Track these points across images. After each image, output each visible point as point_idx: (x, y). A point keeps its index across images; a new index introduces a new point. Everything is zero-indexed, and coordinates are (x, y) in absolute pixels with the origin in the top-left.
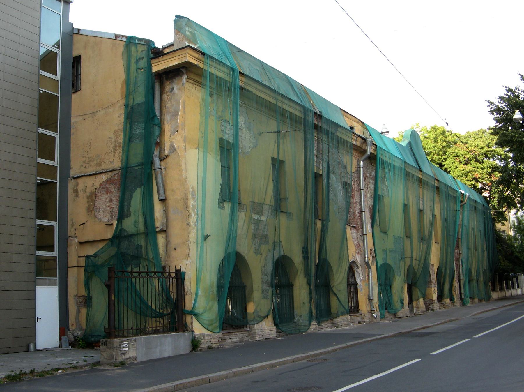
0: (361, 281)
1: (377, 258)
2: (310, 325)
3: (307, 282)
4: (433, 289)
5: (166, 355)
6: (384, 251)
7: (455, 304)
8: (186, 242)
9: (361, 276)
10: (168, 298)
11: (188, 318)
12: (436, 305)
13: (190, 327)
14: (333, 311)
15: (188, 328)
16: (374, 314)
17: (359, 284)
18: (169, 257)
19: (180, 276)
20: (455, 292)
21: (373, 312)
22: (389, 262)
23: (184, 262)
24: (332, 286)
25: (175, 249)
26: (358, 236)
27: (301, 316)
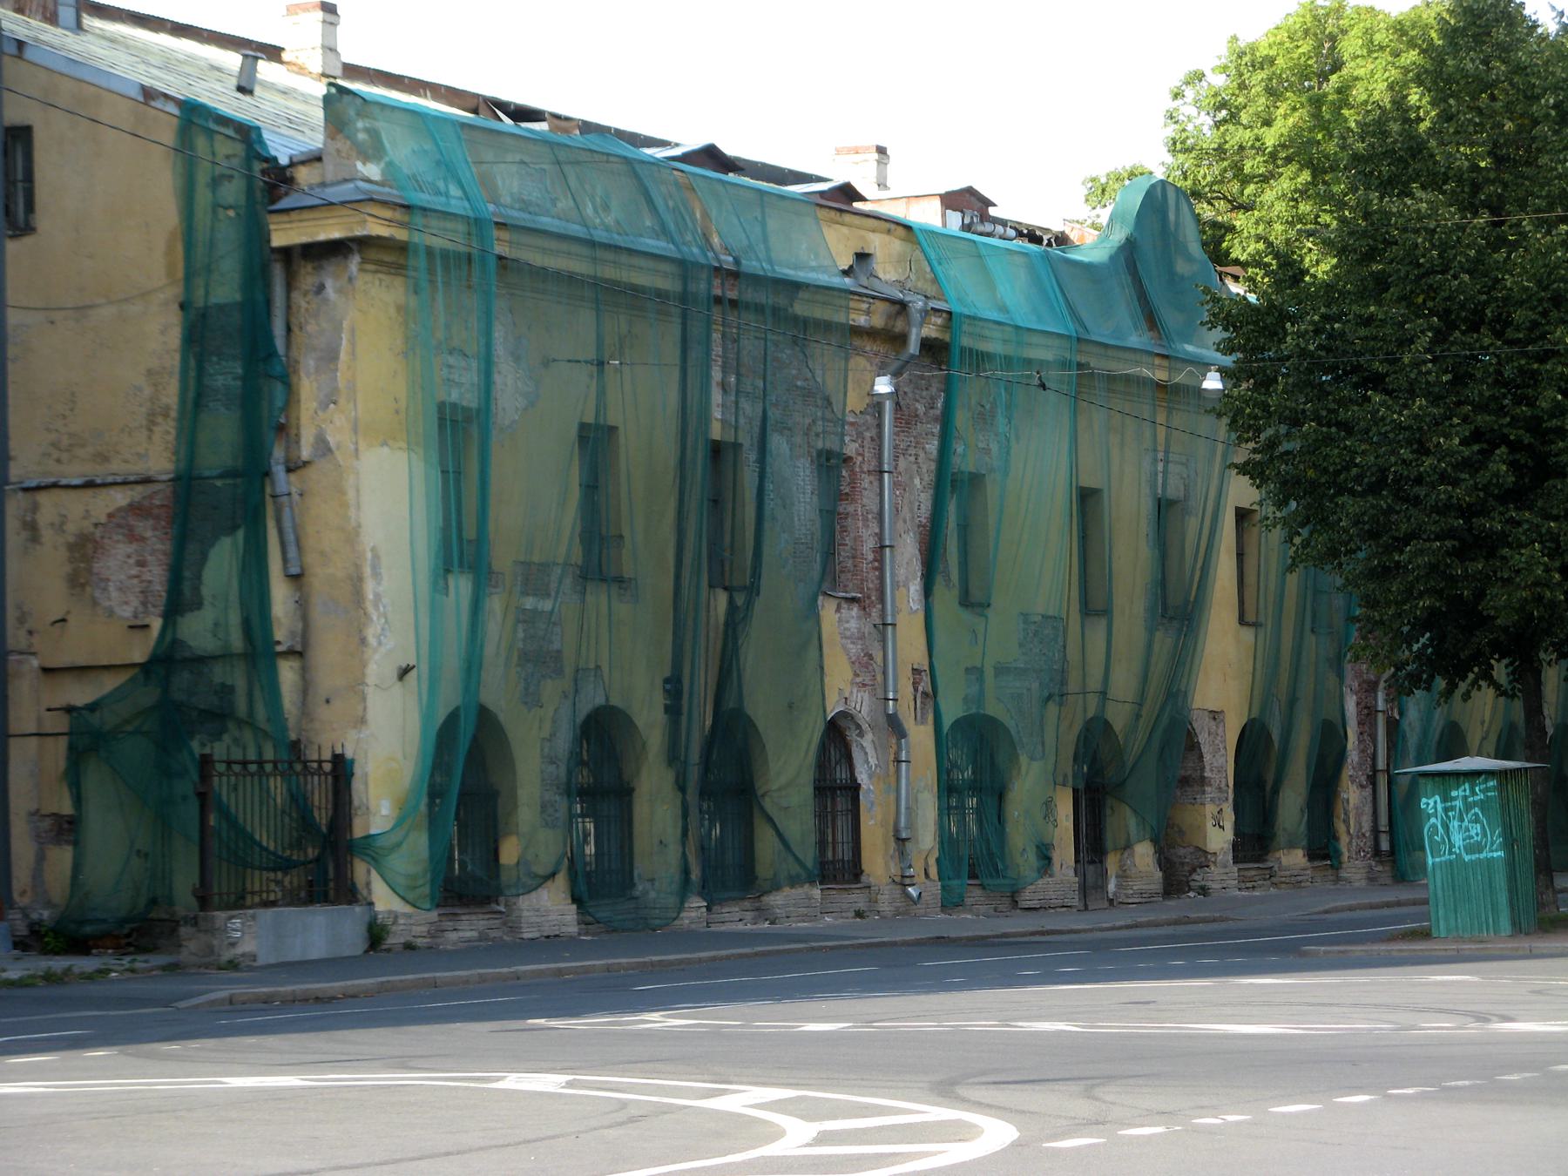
0: (870, 777)
1: (938, 699)
2: (681, 908)
3: (677, 781)
4: (1210, 809)
5: (314, 955)
6: (975, 672)
7: (1343, 874)
8: (357, 687)
9: (873, 761)
10: (305, 821)
11: (360, 869)
12: (1222, 874)
13: (365, 892)
14: (763, 870)
15: (359, 896)
16: (910, 889)
17: (864, 786)
18: (312, 720)
19: (341, 769)
20: (1347, 822)
21: (907, 881)
22: (993, 709)
23: (352, 735)
24: (760, 793)
25: (328, 701)
26: (868, 629)
27: (652, 880)
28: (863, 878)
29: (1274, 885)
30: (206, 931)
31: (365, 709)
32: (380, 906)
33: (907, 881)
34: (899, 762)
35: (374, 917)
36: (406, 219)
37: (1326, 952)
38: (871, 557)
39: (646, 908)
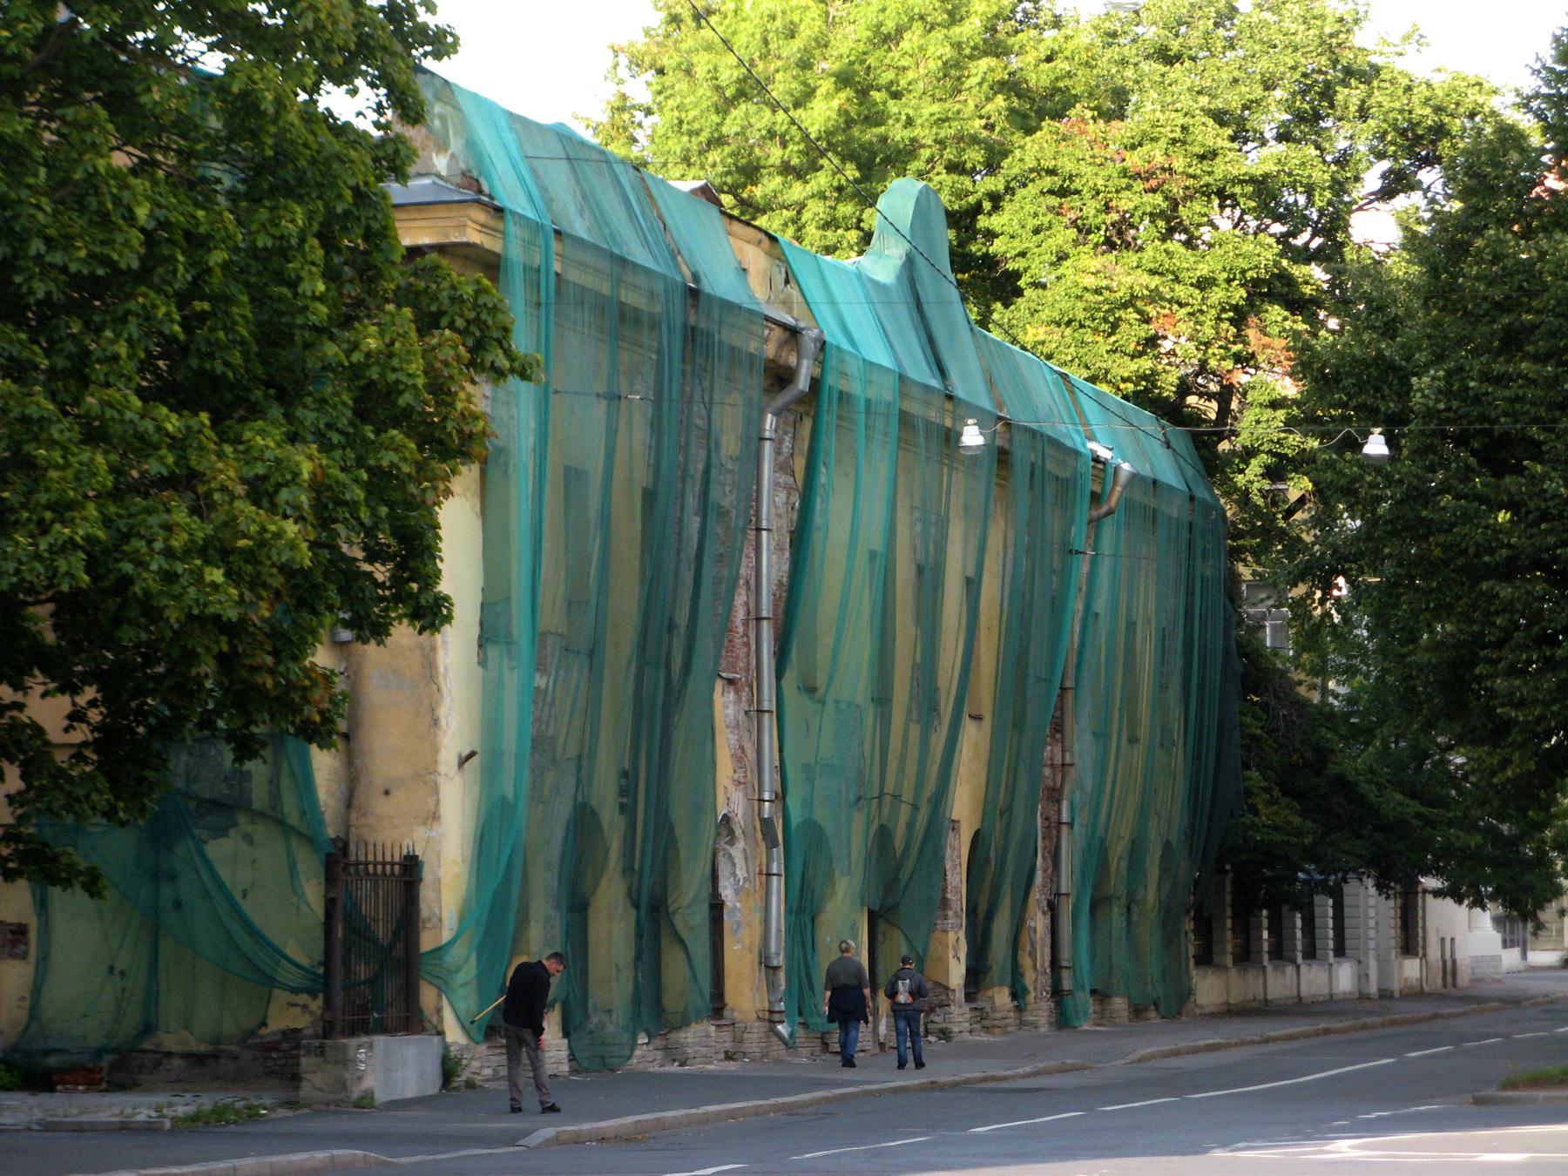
0: (737, 892)
1: (788, 799)
2: (633, 1046)
3: (629, 894)
4: (951, 936)
5: (411, 1092)
6: (808, 769)
7: (1029, 1018)
8: (426, 777)
9: (741, 874)
10: (359, 931)
11: (427, 995)
12: (959, 1015)
13: (434, 1020)
14: (672, 1001)
15: (427, 1025)
16: (780, 1027)
17: (729, 904)
18: (365, 815)
20: (1032, 955)
21: (776, 1017)
22: (822, 816)
23: (420, 833)
24: (671, 909)
25: (387, 793)
26: (742, 717)
27: (609, 1011)
28: (726, 1013)
29: (986, 1029)
30: (336, 1062)
31: (438, 802)
32: (449, 1039)
33: (776, 1017)
34: (769, 875)
35: (446, 1047)
36: (492, 223)
37: (1548, 1099)
38: (741, 630)
39: (603, 1044)
